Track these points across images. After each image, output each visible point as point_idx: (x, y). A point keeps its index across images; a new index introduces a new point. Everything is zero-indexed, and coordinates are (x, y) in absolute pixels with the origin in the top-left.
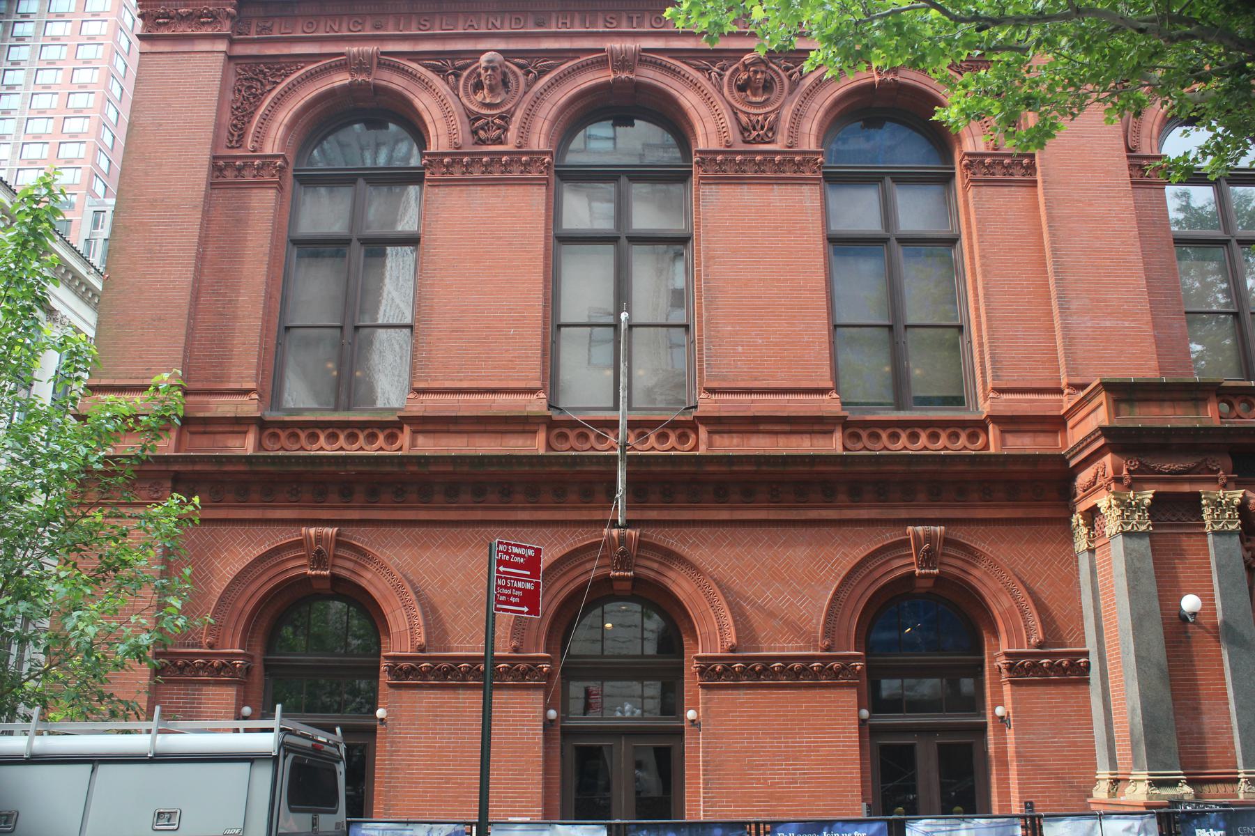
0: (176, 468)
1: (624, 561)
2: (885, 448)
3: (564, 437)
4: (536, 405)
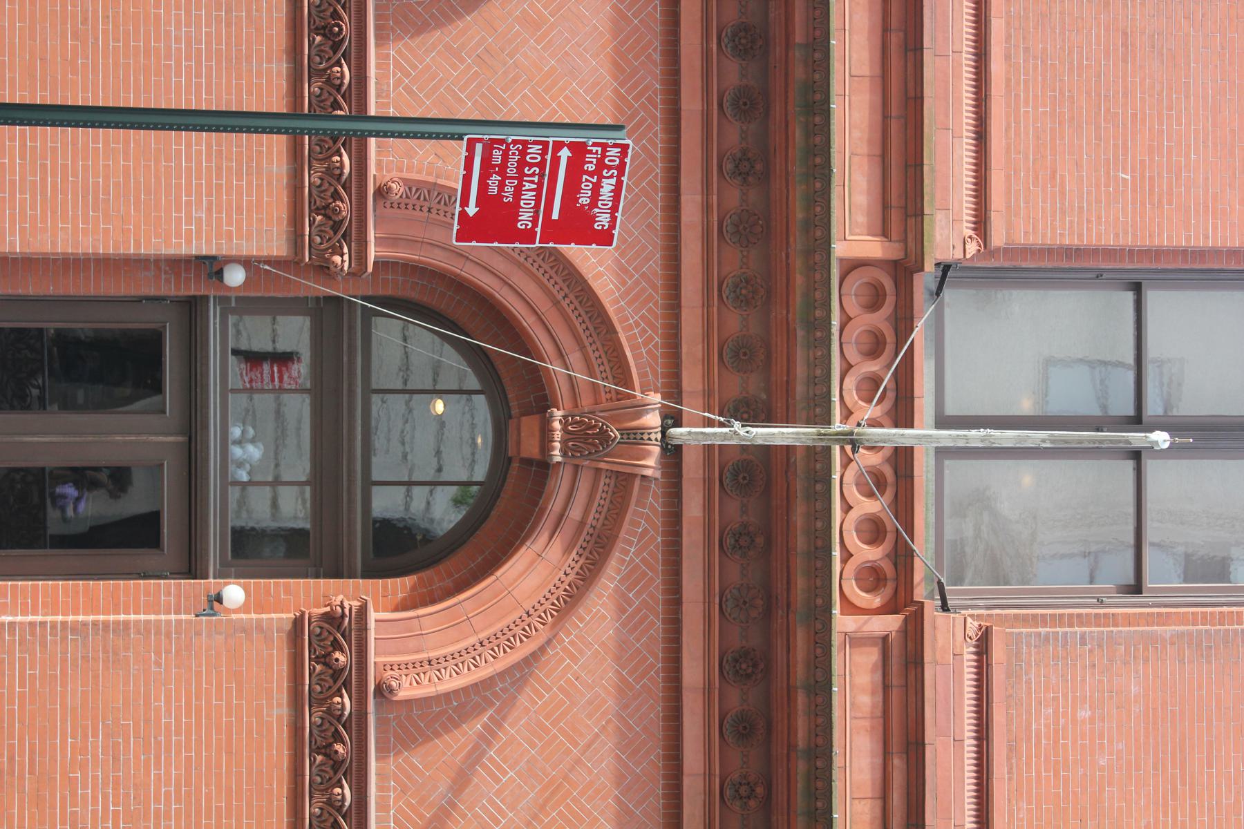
1: (587, 440)
3: (874, 303)
4: (948, 234)
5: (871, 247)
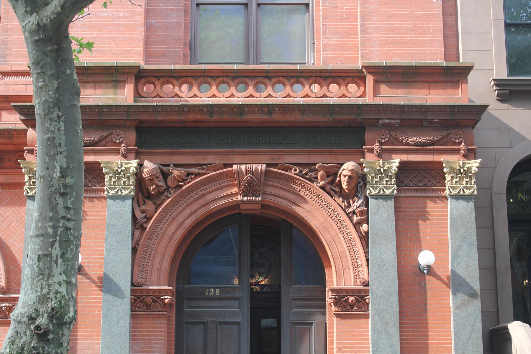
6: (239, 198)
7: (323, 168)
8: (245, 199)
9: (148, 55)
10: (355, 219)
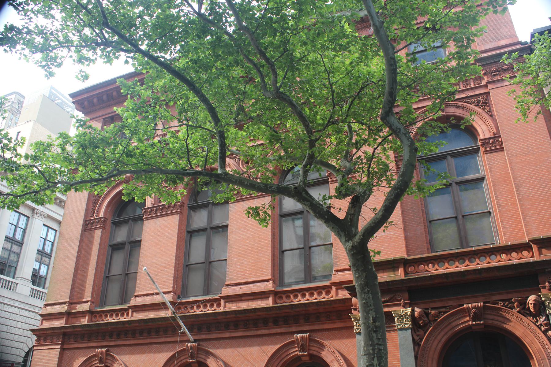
0: (62, 331)
1: (192, 356)
2: (292, 301)
3: (281, 298)
4: (269, 286)
5: (271, 299)
6: (471, 323)
7: (517, 301)
8: (474, 323)
9: (408, 251)
10: (543, 328)
